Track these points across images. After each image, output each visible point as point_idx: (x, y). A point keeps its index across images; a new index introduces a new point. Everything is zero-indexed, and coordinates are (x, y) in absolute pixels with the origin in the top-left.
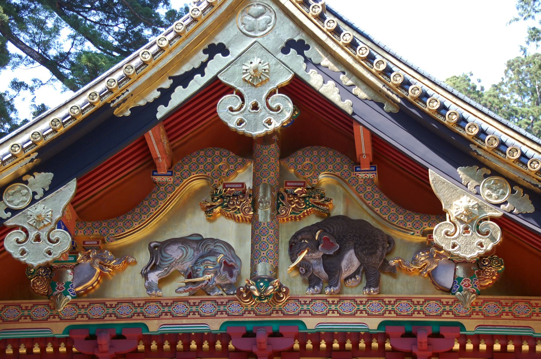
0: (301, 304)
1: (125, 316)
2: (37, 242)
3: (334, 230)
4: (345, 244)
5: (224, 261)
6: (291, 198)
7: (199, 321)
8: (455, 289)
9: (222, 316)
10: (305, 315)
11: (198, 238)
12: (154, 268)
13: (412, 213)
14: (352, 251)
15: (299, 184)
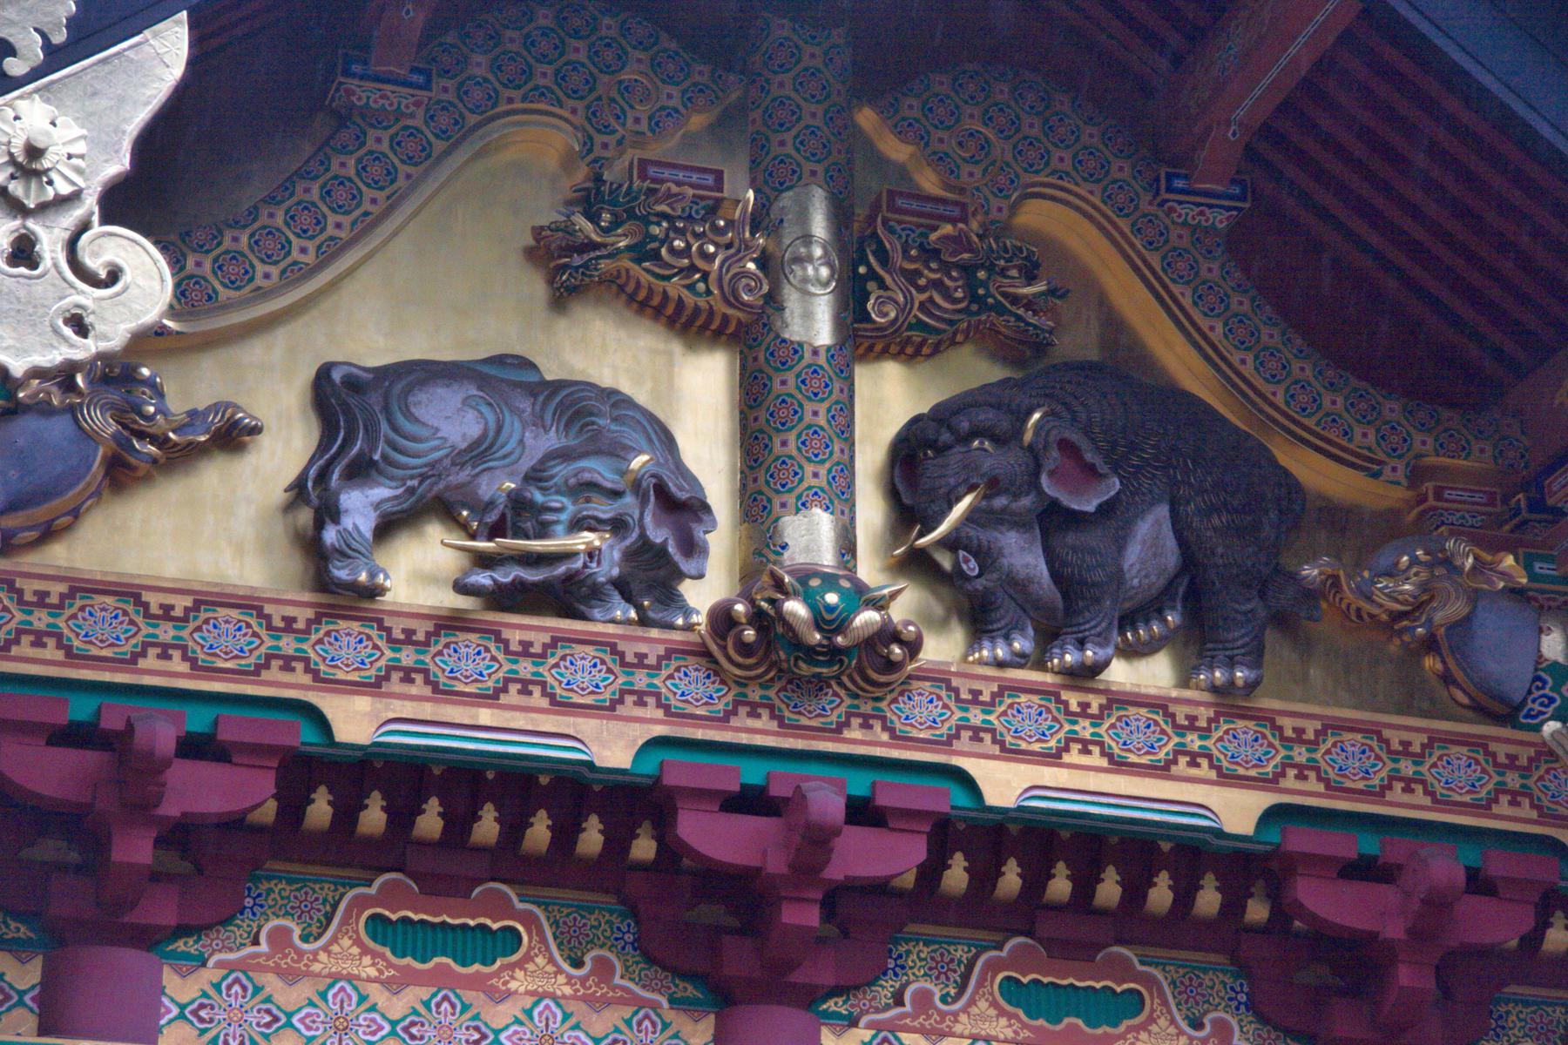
0: (958, 700)
1: (229, 665)
2: (23, 270)
3: (1090, 419)
4: (1137, 479)
5: (654, 481)
6: (912, 260)
7: (549, 723)
8: (1537, 707)
9: (639, 712)
10: (977, 747)
11: (533, 378)
12: (361, 471)
13: (1371, 390)
14: (1163, 511)
15: (941, 209)
